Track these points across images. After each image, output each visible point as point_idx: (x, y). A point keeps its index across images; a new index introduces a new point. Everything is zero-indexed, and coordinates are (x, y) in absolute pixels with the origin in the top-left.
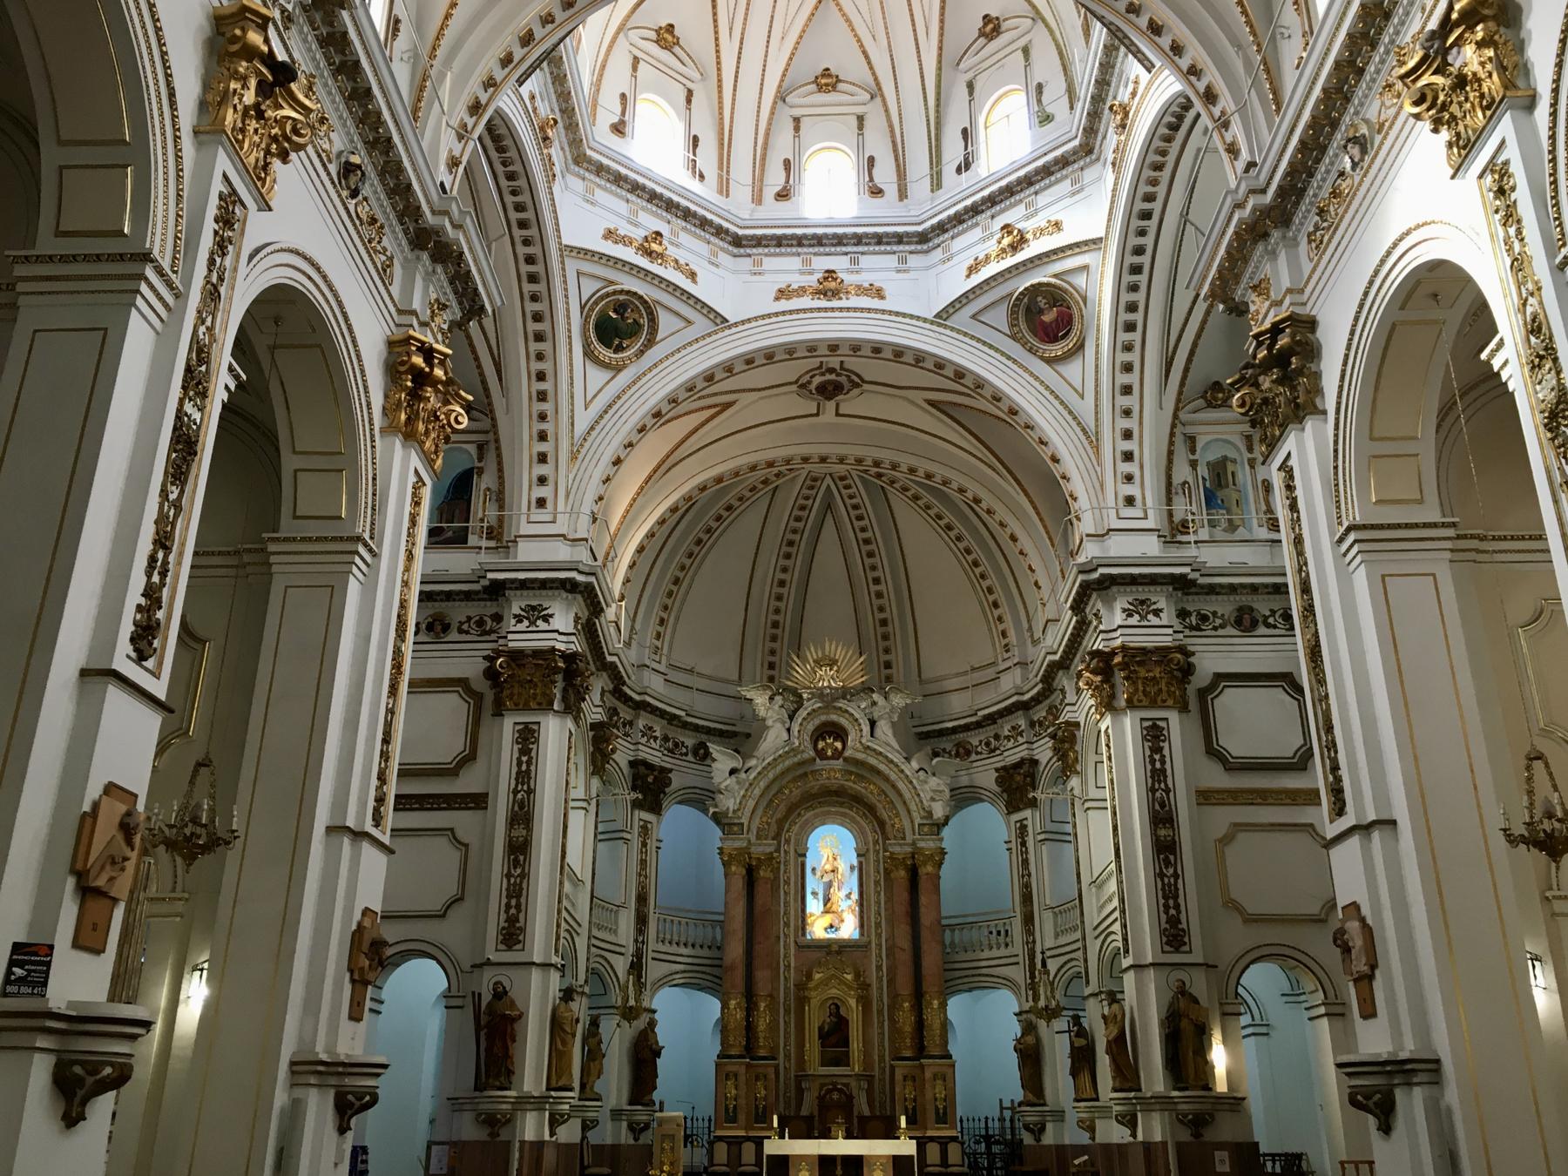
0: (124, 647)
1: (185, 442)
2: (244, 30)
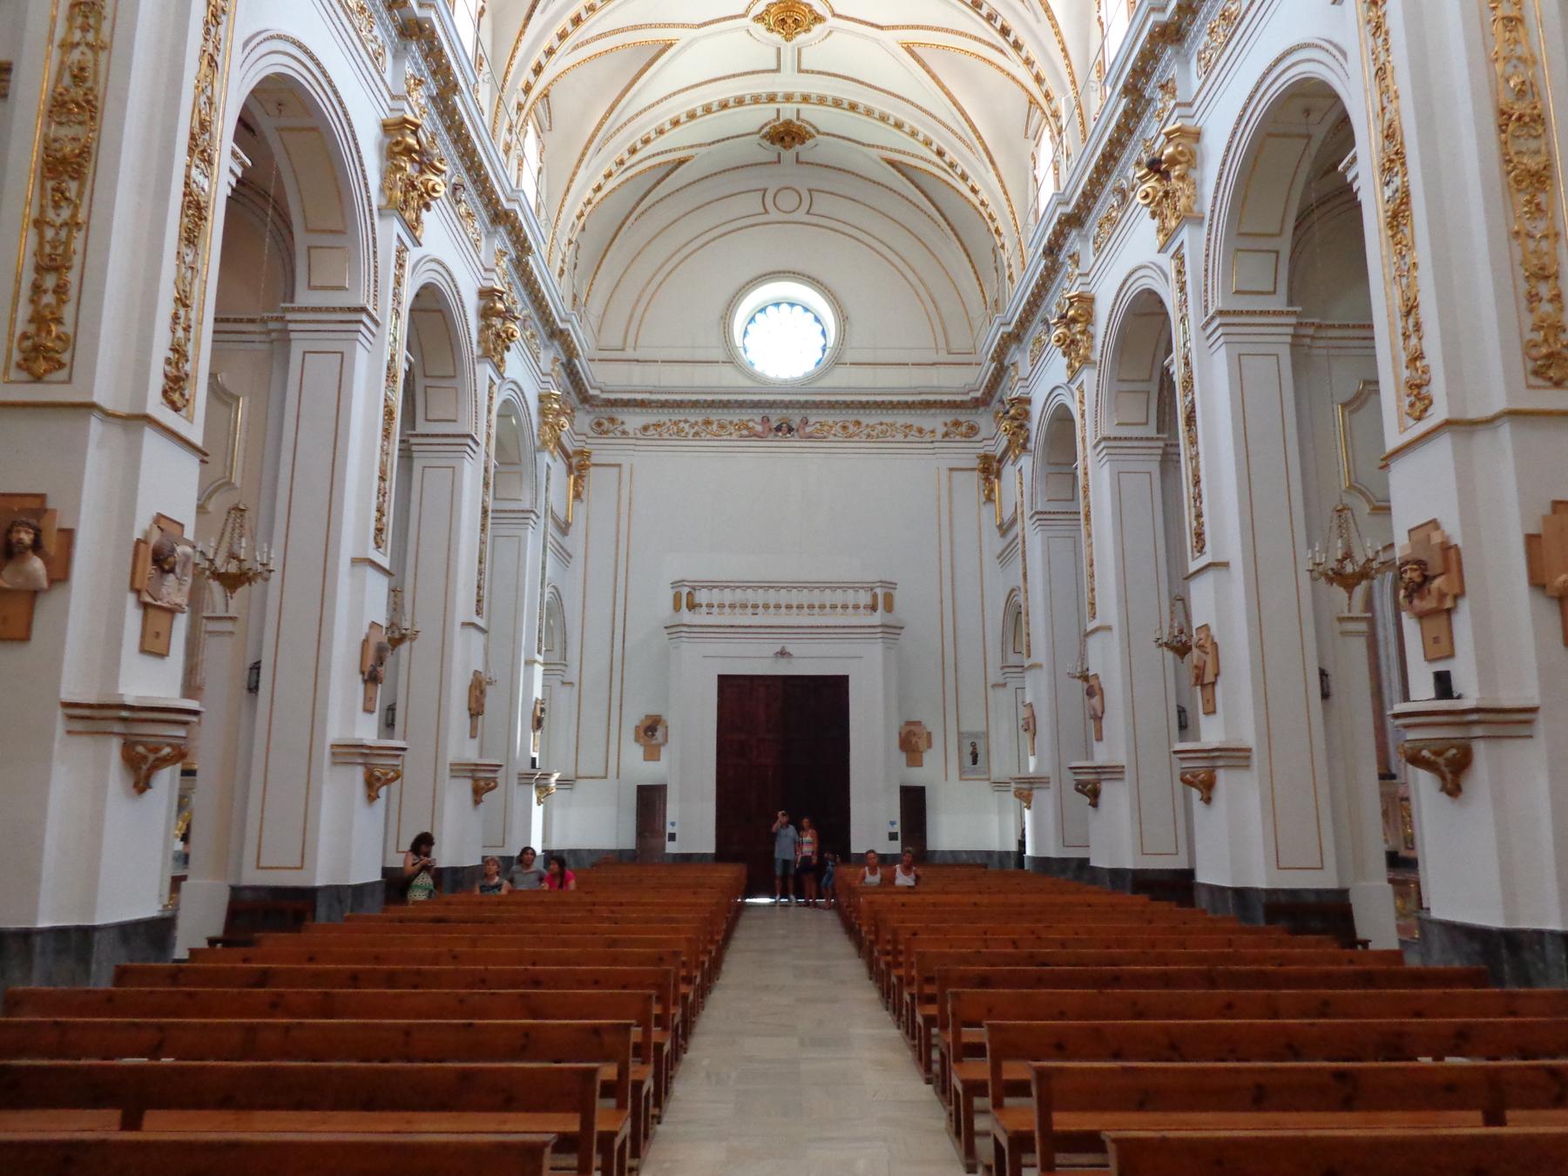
0: (372, 544)
1: (389, 413)
2: (403, 137)
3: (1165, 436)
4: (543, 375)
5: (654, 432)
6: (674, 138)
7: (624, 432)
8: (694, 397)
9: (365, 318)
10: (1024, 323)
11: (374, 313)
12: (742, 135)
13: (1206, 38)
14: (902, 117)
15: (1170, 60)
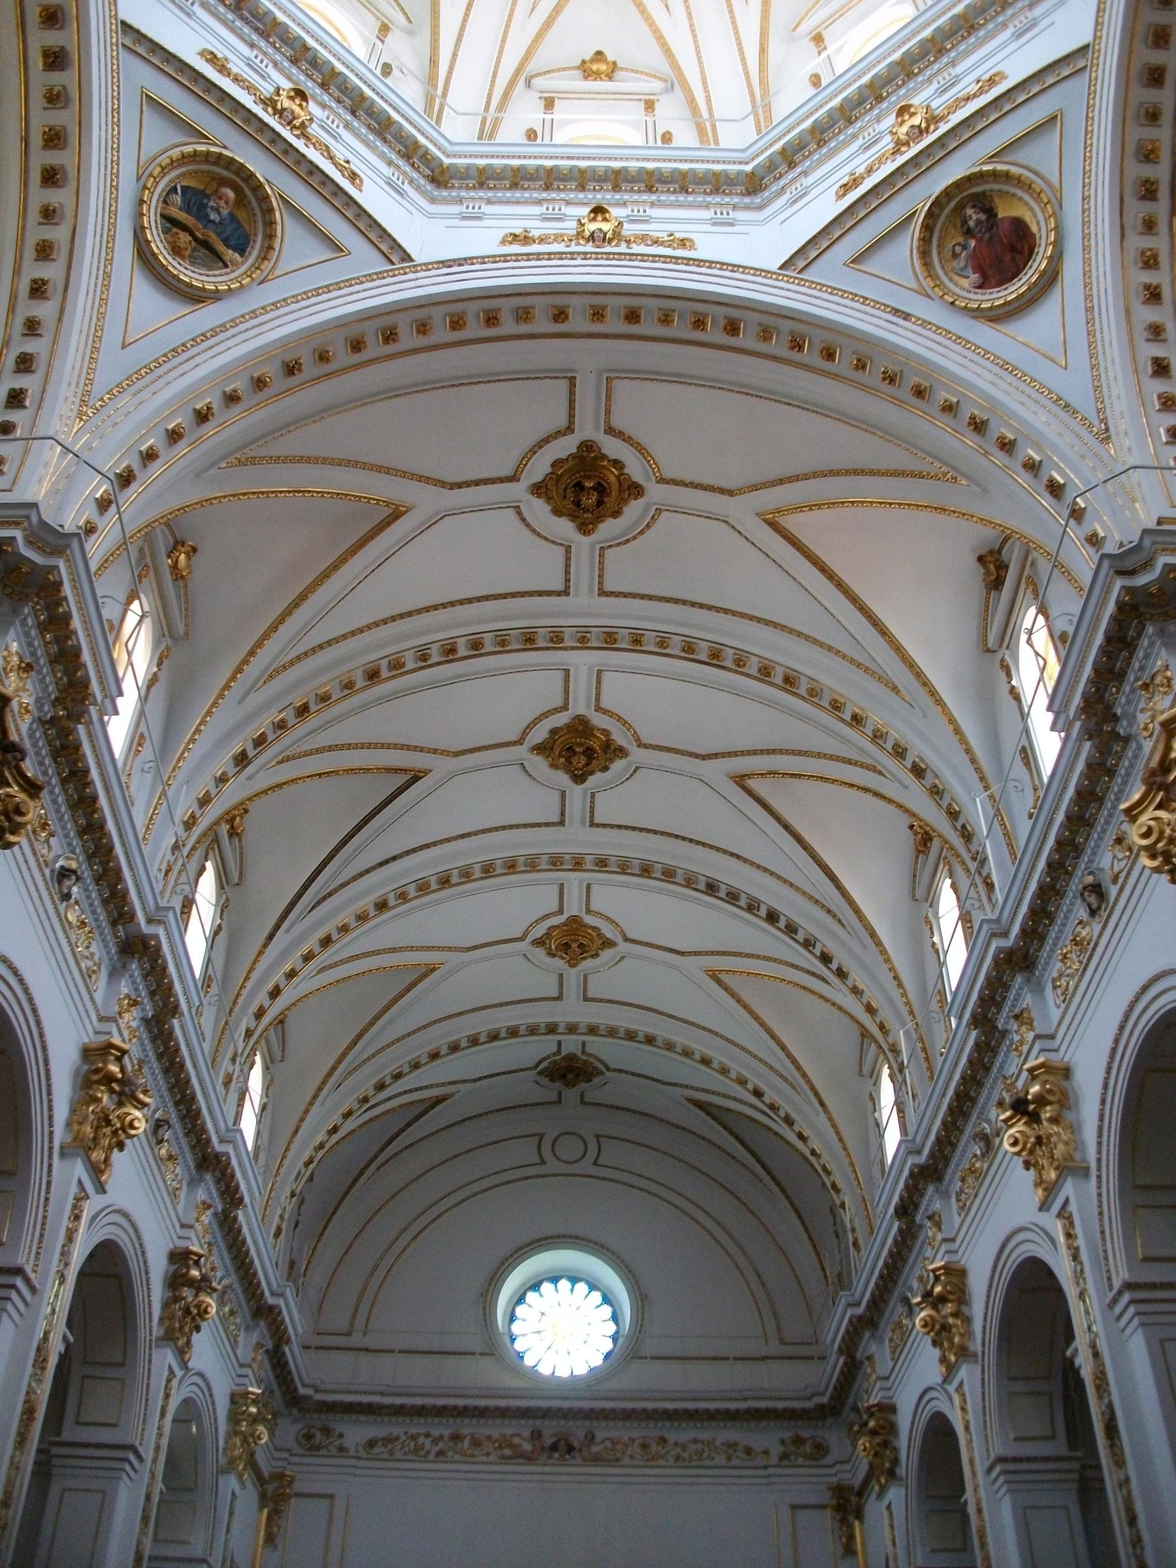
1: (29, 1411)
3: (1079, 1454)
4: (241, 1366)
5: (383, 1449)
6: (435, 1074)
7: (341, 1449)
8: (440, 1402)
9: (19, 1282)
10: (878, 1302)
11: (32, 1276)
12: (515, 1071)
13: (1060, 964)
14: (710, 1053)
15: (1021, 988)
